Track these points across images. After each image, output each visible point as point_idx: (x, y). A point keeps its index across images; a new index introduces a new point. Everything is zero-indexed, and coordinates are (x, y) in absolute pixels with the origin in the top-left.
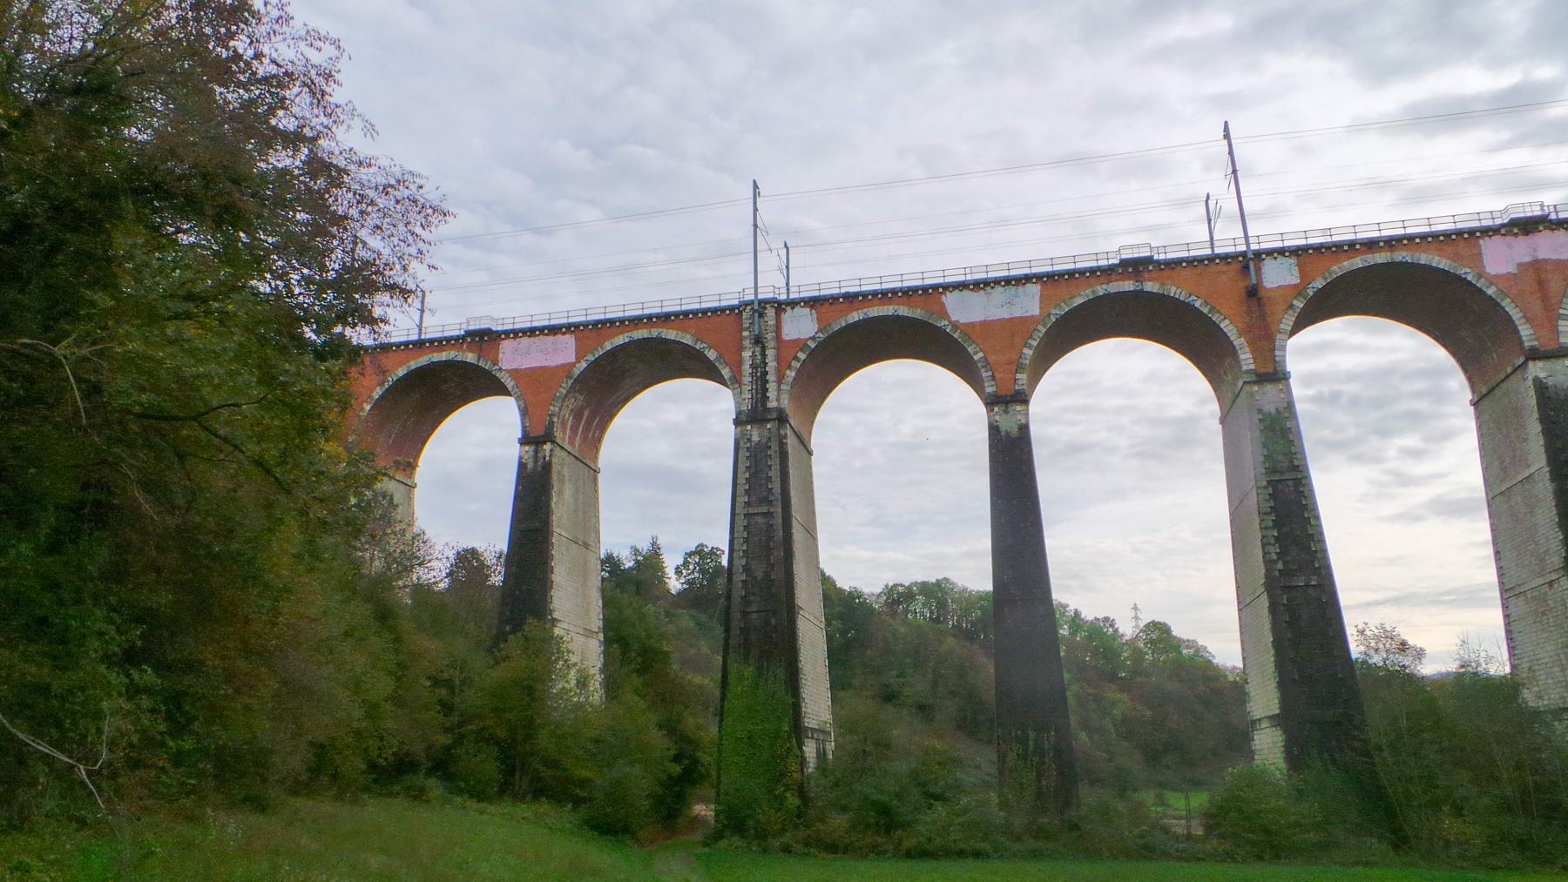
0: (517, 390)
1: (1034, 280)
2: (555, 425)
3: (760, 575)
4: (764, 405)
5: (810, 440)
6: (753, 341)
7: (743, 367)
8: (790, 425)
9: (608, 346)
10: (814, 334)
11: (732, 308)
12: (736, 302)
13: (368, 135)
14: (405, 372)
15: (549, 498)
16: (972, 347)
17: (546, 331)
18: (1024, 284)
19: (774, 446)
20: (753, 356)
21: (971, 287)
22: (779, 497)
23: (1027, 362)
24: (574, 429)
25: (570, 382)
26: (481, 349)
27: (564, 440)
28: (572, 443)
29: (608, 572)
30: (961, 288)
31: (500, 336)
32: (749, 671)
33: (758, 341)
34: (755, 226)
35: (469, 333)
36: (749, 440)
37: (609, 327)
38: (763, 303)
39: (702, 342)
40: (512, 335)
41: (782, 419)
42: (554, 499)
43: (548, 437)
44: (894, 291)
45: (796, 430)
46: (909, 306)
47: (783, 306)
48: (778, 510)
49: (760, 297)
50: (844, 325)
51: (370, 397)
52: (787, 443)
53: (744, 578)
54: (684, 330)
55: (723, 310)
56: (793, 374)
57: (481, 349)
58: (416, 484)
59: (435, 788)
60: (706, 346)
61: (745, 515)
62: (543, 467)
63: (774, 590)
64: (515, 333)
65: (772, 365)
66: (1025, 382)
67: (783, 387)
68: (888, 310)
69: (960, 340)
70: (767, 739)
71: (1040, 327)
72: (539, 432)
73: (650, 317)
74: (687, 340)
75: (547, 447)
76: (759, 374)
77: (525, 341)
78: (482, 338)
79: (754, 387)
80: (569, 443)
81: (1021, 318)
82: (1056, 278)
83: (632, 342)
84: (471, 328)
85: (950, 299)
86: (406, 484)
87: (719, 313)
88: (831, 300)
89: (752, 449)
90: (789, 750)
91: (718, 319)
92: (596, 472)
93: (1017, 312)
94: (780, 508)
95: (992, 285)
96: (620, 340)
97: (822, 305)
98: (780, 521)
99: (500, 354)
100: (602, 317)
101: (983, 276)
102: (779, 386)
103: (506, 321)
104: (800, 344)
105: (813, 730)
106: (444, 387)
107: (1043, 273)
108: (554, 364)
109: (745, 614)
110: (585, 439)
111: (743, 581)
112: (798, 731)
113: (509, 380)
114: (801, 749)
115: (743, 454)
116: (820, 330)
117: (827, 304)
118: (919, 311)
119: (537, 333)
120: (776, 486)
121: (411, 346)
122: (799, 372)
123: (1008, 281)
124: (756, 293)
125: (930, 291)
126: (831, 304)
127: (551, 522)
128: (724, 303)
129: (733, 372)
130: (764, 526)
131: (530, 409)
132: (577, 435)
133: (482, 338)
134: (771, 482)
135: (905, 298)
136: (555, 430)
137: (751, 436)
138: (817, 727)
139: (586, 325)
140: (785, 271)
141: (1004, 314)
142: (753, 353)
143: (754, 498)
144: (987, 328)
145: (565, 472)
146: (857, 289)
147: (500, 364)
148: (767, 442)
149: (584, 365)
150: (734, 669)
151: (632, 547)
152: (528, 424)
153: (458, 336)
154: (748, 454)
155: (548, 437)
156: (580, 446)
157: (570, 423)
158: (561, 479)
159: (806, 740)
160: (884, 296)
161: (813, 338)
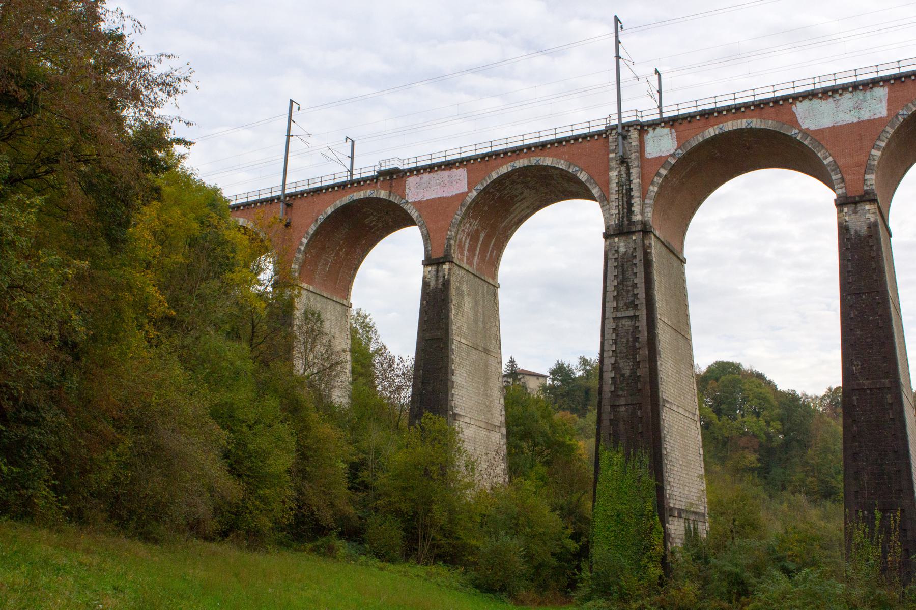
0: (420, 219)
1: (881, 84)
2: (453, 247)
3: (627, 372)
4: (630, 219)
5: (682, 249)
6: (618, 162)
8: (655, 236)
9: (494, 176)
10: (674, 151)
11: (600, 133)
12: (603, 128)
13: (137, 30)
14: (333, 210)
15: (448, 311)
16: (822, 152)
17: (443, 167)
18: (871, 88)
19: (639, 255)
20: (619, 176)
21: (820, 95)
22: (644, 302)
23: (876, 163)
24: (472, 250)
25: (464, 209)
26: (391, 187)
27: (462, 260)
28: (470, 263)
29: (561, 381)
30: (810, 97)
31: (406, 173)
32: (618, 458)
33: (623, 161)
34: (618, 57)
35: (381, 174)
36: (617, 251)
38: (627, 126)
40: (415, 173)
41: (646, 231)
42: (454, 312)
43: (446, 258)
44: (747, 105)
45: (663, 240)
46: (761, 117)
47: (646, 128)
48: (643, 313)
49: (624, 121)
50: (701, 140)
51: (307, 233)
52: (651, 253)
53: (613, 376)
54: (558, 156)
55: (591, 135)
56: (656, 189)
57: (391, 187)
58: (351, 304)
59: (342, 547)
60: (577, 169)
61: (613, 318)
62: (443, 284)
63: (639, 386)
64: (417, 171)
65: (636, 182)
66: (874, 182)
67: (647, 201)
68: (742, 123)
69: (810, 147)
70: (633, 516)
71: (888, 129)
72: (438, 254)
73: (529, 147)
74: (562, 165)
75: (446, 267)
76: (624, 191)
77: (426, 177)
78: (391, 178)
79: (621, 203)
80: (467, 263)
81: (868, 121)
82: (903, 79)
83: (514, 171)
84: (383, 168)
85: (800, 109)
86: (343, 305)
87: (589, 139)
88: (690, 118)
89: (620, 259)
90: (652, 528)
91: (588, 144)
92: (496, 287)
93: (865, 115)
94: (645, 310)
95: (840, 92)
96: (504, 169)
97: (681, 123)
98: (644, 323)
99: (407, 189)
100: (489, 150)
101: (832, 83)
102: (644, 201)
103: (410, 161)
104: (661, 161)
105: (680, 511)
106: (367, 221)
107: (890, 75)
108: (450, 195)
109: (614, 407)
110: (482, 258)
111: (612, 378)
112: (662, 510)
113: (413, 213)
114: (664, 526)
115: (612, 264)
116: (679, 148)
117: (685, 123)
118: (770, 122)
119: (436, 168)
120: (641, 291)
121: (336, 188)
122: (661, 187)
123: (855, 87)
124: (620, 118)
125: (781, 102)
126: (689, 122)
127: (450, 331)
128: (593, 130)
130: (631, 328)
131: (431, 235)
132: (475, 255)
133: (391, 178)
134: (637, 288)
135: (758, 110)
136: (452, 251)
137: (618, 247)
138: (684, 508)
139: (475, 158)
140: (657, 96)
141: (851, 118)
142: (619, 172)
143: (621, 304)
144: (835, 131)
145: (464, 288)
146: (713, 106)
147: (406, 199)
148: (633, 252)
149: (475, 193)
150: (605, 455)
151: (581, 358)
152: (430, 248)
153: (373, 176)
154: (616, 264)
155: (446, 258)
156: (478, 264)
157: (467, 245)
158: (461, 294)
159: (670, 519)
160: (737, 110)
161: (673, 155)
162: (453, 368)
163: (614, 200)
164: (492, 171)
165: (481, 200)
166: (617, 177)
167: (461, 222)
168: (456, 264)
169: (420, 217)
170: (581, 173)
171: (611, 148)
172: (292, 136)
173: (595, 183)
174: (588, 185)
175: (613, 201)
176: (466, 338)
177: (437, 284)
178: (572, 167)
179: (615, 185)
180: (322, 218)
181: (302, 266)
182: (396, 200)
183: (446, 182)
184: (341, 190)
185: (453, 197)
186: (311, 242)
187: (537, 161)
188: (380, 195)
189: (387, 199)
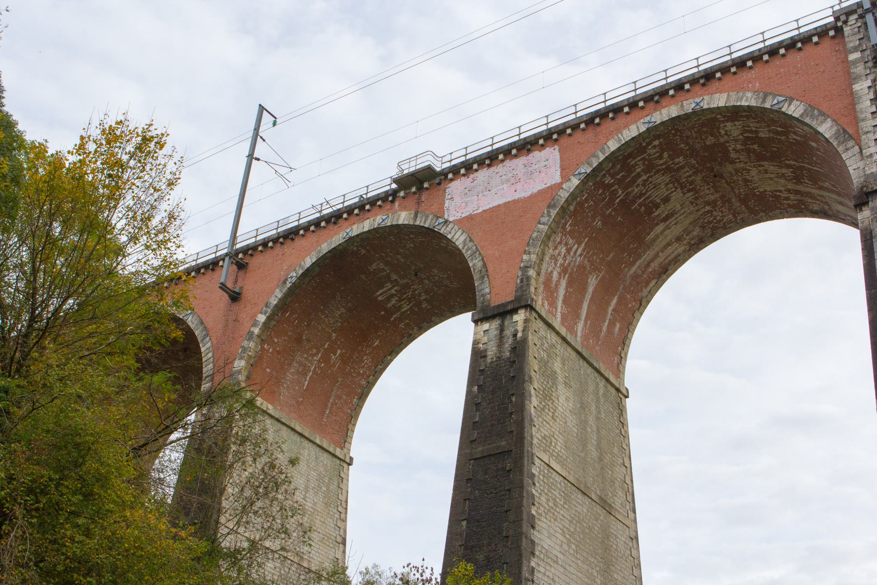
0: (470, 244)
2: (533, 282)
6: (870, 64)
7: (858, 107)
9: (613, 145)
11: (822, 33)
15: (523, 396)
17: (514, 151)
25: (554, 212)
31: (446, 175)
37: (613, 119)
39: (775, 96)
40: (463, 171)
57: (419, 203)
58: (351, 459)
60: (781, 99)
62: (514, 349)
64: (467, 167)
74: (749, 100)
75: (520, 317)
77: (482, 175)
83: (653, 132)
86: (334, 455)
87: (799, 45)
96: (632, 131)
106: (380, 295)
113: (456, 237)
119: (501, 157)
129: (837, 124)
131: (490, 269)
136: (532, 290)
147: (446, 217)
149: (575, 182)
157: (562, 292)
162: (533, 512)
163: (871, 129)
164: (608, 140)
165: (587, 200)
166: (872, 90)
167: (548, 237)
168: (540, 316)
169: (471, 240)
170: (790, 104)
171: (852, 45)
172: (258, 159)
173: (822, 114)
174: (807, 120)
175: (867, 132)
176: (558, 458)
177: (500, 352)
178: (770, 98)
179: (868, 103)
180: (294, 275)
181: (254, 365)
182: (427, 223)
183: (520, 176)
184: (331, 226)
185: (532, 197)
186: (273, 323)
187: (697, 104)
188: (398, 220)
189: (411, 223)
